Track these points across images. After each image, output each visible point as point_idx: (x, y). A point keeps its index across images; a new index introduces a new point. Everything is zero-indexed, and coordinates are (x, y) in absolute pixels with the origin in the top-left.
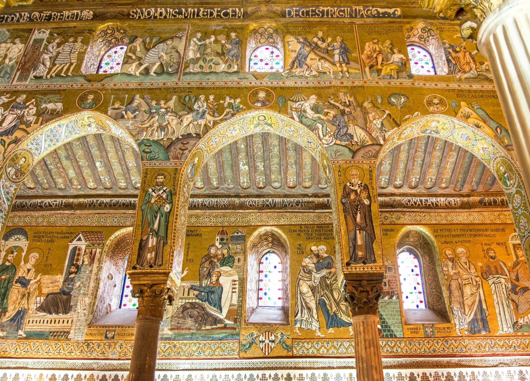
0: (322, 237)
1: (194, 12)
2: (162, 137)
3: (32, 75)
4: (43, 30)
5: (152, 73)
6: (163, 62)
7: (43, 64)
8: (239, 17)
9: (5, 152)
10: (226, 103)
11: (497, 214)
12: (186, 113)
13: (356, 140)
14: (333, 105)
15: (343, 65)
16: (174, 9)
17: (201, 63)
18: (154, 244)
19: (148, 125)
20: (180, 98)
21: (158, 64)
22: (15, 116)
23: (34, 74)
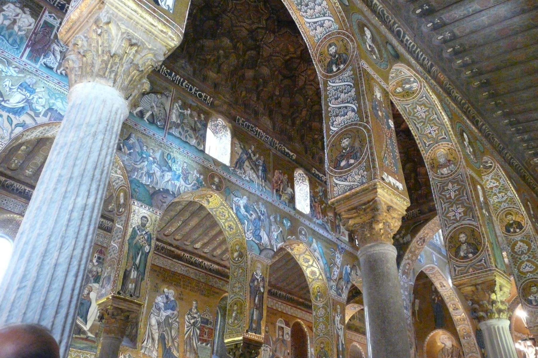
0: (174, 283)
1: (180, 80)
2: (149, 183)
3: (42, 60)
4: (53, 15)
5: (145, 119)
6: (154, 114)
7: (54, 54)
8: (208, 104)
9: (11, 133)
10: (194, 175)
11: (275, 301)
12: (167, 169)
13: (263, 242)
14: (256, 210)
15: (263, 181)
16: (167, 69)
17: (180, 129)
18: (135, 277)
19: (139, 167)
20: (163, 154)
21: (149, 113)
22: (24, 97)
23: (45, 60)
